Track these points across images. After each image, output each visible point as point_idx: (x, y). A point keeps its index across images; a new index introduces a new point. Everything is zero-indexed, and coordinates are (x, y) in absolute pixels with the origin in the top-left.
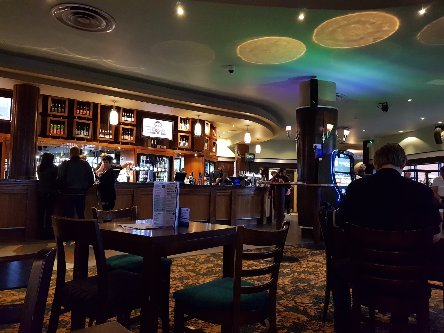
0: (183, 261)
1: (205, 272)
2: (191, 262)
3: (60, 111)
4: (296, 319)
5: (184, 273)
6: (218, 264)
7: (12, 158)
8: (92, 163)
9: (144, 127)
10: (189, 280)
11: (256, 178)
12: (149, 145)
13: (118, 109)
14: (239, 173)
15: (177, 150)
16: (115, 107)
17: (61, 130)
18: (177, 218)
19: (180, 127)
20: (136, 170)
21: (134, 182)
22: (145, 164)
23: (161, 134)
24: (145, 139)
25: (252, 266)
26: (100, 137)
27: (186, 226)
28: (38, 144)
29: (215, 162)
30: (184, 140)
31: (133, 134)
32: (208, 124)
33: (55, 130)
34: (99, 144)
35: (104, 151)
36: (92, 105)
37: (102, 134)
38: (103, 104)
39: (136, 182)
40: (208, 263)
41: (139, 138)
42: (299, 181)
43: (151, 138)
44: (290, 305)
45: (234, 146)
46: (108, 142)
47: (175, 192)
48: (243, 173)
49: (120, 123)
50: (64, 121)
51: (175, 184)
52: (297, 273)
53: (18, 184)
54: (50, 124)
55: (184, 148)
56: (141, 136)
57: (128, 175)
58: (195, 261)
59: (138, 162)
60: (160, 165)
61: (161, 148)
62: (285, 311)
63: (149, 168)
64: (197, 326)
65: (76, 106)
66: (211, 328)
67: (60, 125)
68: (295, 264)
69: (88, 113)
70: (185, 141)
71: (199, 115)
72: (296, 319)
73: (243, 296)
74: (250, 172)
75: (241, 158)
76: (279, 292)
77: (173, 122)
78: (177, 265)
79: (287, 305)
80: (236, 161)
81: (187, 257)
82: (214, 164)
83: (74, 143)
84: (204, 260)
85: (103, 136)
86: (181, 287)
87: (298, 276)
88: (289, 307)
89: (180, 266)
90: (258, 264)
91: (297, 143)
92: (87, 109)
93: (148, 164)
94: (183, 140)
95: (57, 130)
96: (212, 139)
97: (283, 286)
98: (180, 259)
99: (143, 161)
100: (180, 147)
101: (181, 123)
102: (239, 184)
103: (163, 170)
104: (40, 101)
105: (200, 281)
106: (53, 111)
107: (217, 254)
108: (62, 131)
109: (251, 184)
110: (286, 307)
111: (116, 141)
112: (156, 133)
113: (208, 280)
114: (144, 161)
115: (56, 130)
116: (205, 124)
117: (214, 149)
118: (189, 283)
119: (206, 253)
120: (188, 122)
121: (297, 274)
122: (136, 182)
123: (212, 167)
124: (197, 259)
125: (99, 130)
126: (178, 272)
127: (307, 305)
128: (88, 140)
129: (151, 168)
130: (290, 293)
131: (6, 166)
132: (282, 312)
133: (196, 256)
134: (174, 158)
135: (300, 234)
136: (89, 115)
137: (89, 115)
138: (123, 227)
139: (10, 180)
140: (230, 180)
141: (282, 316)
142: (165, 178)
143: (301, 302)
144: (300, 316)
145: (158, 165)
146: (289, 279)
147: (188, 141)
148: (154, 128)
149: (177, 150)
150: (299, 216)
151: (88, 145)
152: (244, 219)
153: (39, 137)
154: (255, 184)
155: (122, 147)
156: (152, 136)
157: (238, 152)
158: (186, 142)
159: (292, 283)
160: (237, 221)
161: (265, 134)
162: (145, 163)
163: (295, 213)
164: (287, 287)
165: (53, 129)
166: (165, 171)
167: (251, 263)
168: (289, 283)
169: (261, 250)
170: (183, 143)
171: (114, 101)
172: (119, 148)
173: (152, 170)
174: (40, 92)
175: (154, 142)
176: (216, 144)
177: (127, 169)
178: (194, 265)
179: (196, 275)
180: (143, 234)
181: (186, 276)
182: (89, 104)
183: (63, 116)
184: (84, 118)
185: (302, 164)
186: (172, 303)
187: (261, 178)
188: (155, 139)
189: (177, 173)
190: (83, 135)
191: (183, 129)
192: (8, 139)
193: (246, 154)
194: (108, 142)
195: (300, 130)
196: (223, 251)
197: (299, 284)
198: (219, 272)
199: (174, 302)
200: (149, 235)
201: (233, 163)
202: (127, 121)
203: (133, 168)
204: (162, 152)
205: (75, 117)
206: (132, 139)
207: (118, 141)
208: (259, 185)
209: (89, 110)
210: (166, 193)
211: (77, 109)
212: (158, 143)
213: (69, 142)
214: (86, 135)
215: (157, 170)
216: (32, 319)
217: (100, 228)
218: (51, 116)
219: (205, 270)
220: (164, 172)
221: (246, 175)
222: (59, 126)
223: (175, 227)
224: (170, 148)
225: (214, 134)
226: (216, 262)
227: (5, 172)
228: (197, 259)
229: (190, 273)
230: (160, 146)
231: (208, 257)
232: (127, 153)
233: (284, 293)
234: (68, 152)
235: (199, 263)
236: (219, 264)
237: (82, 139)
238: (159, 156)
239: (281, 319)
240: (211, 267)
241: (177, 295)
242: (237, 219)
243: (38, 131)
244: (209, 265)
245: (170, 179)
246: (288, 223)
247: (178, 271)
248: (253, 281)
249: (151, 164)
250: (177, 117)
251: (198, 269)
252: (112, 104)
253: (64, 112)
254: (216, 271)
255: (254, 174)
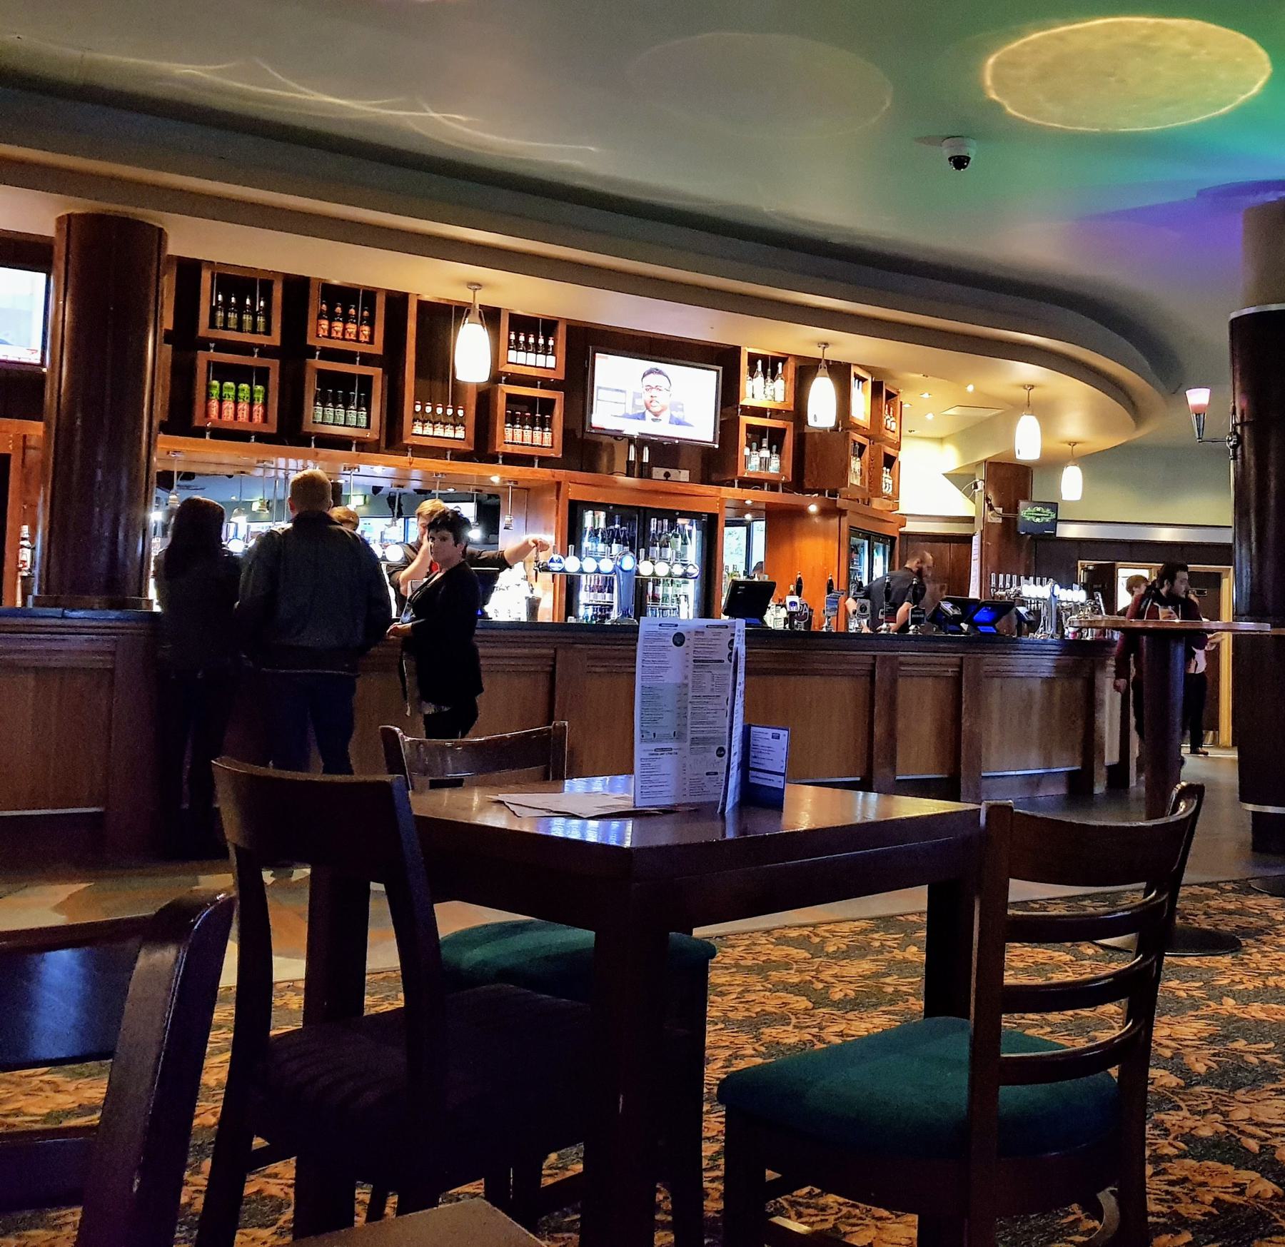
0: (758, 949)
1: (853, 993)
2: (793, 952)
3: (247, 327)
4: (1230, 1190)
5: (763, 1000)
6: (905, 961)
7: (51, 522)
8: (382, 540)
9: (600, 391)
10: (785, 1028)
11: (1064, 604)
12: (620, 465)
13: (491, 316)
14: (993, 583)
15: (734, 487)
16: (477, 307)
17: (251, 404)
18: (734, 772)
19: (749, 394)
20: (563, 570)
21: (556, 621)
22: (601, 547)
23: (670, 423)
24: (601, 443)
25: (1047, 967)
26: (415, 432)
27: (773, 802)
28: (158, 465)
29: (893, 539)
30: (764, 445)
31: (550, 420)
32: (863, 380)
34: (411, 463)
35: (430, 491)
36: (380, 302)
37: (424, 422)
38: (426, 297)
39: (566, 620)
40: (863, 957)
41: (579, 437)
42: (1244, 618)
43: (624, 437)
44: (1206, 1132)
45: (972, 472)
46: (449, 453)
47: (727, 661)
48: (1008, 585)
49: (496, 377)
50: (268, 369)
51: (727, 627)
52: (1234, 998)
53: (75, 627)
54: (208, 380)
55: (764, 478)
56: (584, 430)
57: (532, 592)
58: (808, 951)
59: (573, 535)
60: (666, 552)
61: (667, 480)
62: (1183, 1155)
63: (621, 560)
64: (818, 1218)
65: (316, 304)
66: (877, 1227)
67: (251, 385)
68: (1227, 960)
69: (366, 333)
70: (770, 448)
71: (825, 341)
72: (1230, 1190)
73: (1012, 1095)
74: (1038, 579)
75: (1000, 521)
76: (1161, 1077)
77: (718, 371)
78: (737, 965)
79: (1193, 1132)
80: (978, 532)
81: (776, 934)
82: (888, 547)
83: (306, 458)
84: (847, 945)
86: (752, 1056)
87: (1235, 1012)
88: (1201, 1139)
89: (750, 969)
90: (1071, 961)
91: (1235, 458)
92: (362, 316)
93: (615, 546)
94: (759, 448)
95: (236, 403)
96: (883, 441)
97: (1177, 1054)
98: (747, 942)
99: (595, 532)
100: (746, 475)
101: (752, 373)
102: (991, 629)
103: (678, 570)
104: (168, 284)
105: (831, 1030)
106: (218, 325)
107: (901, 918)
108: (258, 409)
109: (1041, 629)
110: (1190, 1138)
111: (482, 450)
112: (649, 416)
113: (863, 1025)
114: (600, 535)
115: (232, 405)
116: (853, 379)
117: (891, 482)
118: (786, 1041)
119: (856, 916)
120: (780, 371)
121: (1231, 1002)
122: (563, 622)
123: (879, 558)
124: (817, 940)
125: (410, 405)
126: (739, 993)
127: (1274, 1130)
128: (363, 446)
129: (628, 563)
130: (1205, 1079)
131: (25, 555)
132: (1169, 1158)
133: (814, 926)
134: (721, 523)
135: (1247, 834)
136: (371, 341)
137: (371, 341)
138: (512, 807)
139: (40, 611)
140: (956, 613)
141: (1172, 1177)
142: (683, 605)
143: (1250, 1119)
144: (1245, 1176)
145: (658, 548)
146: (1200, 1024)
147: (779, 452)
148: (639, 396)
149: (734, 487)
150: (1243, 764)
151: (364, 469)
152: (1013, 773)
153: (161, 436)
154: (1060, 627)
155: (508, 477)
156: (633, 429)
157: (990, 495)
158: (771, 453)
159: (1212, 1040)
160: (985, 783)
161: (1101, 422)
162: (603, 540)
163: (1226, 748)
164: (1193, 1058)
165: (221, 401)
166: (685, 575)
167: (1040, 956)
168: (1200, 1039)
169: (1086, 903)
170: (761, 458)
171: (476, 285)
172: (496, 479)
173: (630, 571)
174: (166, 248)
175: (639, 453)
176: (896, 464)
177: (527, 564)
178: (804, 966)
179: (813, 1008)
180: (592, 838)
181: (773, 1010)
182: (369, 295)
183: (260, 346)
184: (348, 357)
185: (1254, 545)
186: (714, 1123)
187: (1082, 604)
188: (641, 442)
189: (735, 584)
190: (344, 425)
191: (760, 402)
192: (32, 442)
193: (1022, 503)
194: (449, 453)
195: (1245, 404)
196: (924, 906)
197: (1241, 1044)
198: (910, 994)
199: (723, 1120)
200: (617, 842)
201: (967, 539)
202: (525, 365)
203: (552, 561)
204: (673, 498)
205: (313, 349)
206: (547, 443)
207: (490, 451)
208: (1074, 633)
209: (371, 322)
210: (691, 664)
211: (320, 317)
212: (655, 461)
213: (287, 456)
214: (356, 427)
215: (650, 573)
216: (135, 1189)
217: (415, 813)
218: (212, 345)
219: (852, 986)
220: (681, 580)
221: (1020, 593)
222: (245, 386)
223: (728, 808)
224: (706, 480)
225: (889, 422)
226: (899, 955)
227: (23, 578)
228: (817, 940)
229: (791, 998)
230: (663, 471)
231: (863, 932)
232: (528, 497)
233: (1179, 1080)
234: (280, 495)
235: (827, 955)
236: (911, 962)
237: (342, 443)
238: (661, 514)
239: (1166, 1187)
240: (876, 975)
241: (733, 1089)
242: (983, 774)
243: (158, 408)
244: (866, 966)
245: (706, 607)
246: (1195, 792)
247: (740, 989)
248: (1051, 1032)
249: (625, 545)
250: (736, 350)
251: (822, 981)
252: (464, 295)
253: (268, 331)
254: (896, 991)
255: (1057, 587)
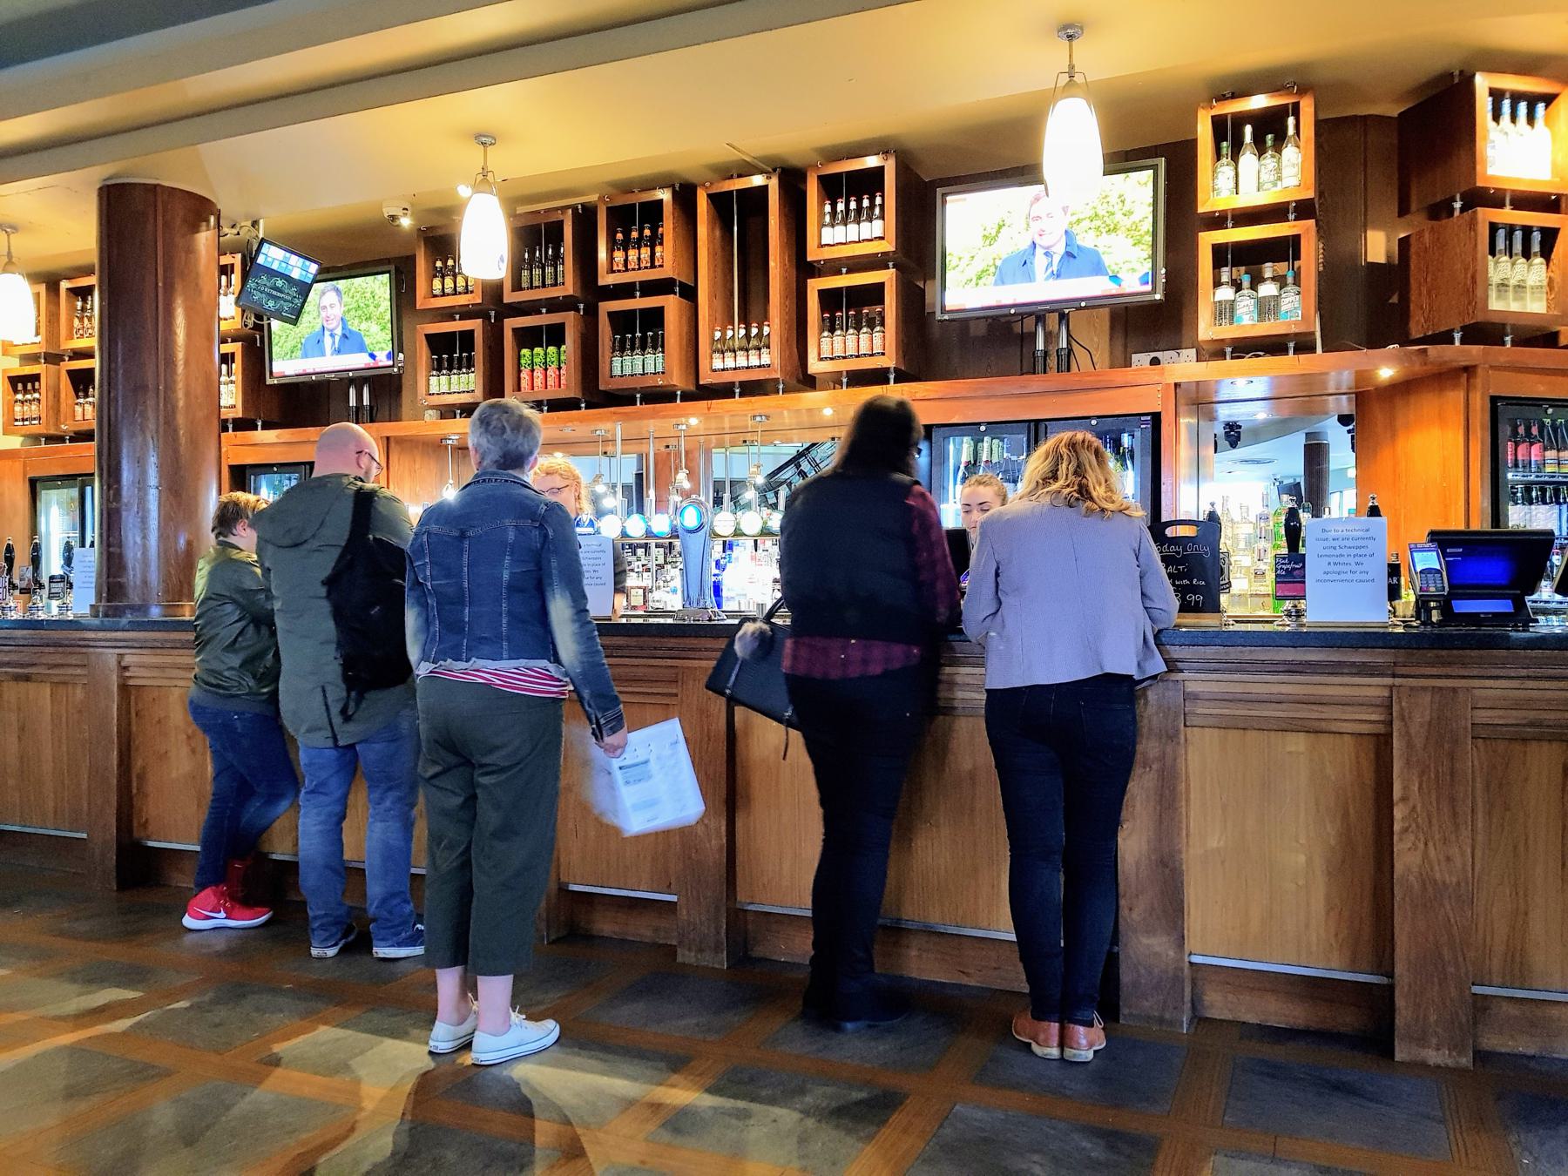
33: (538, 374)
85: (730, 363)
